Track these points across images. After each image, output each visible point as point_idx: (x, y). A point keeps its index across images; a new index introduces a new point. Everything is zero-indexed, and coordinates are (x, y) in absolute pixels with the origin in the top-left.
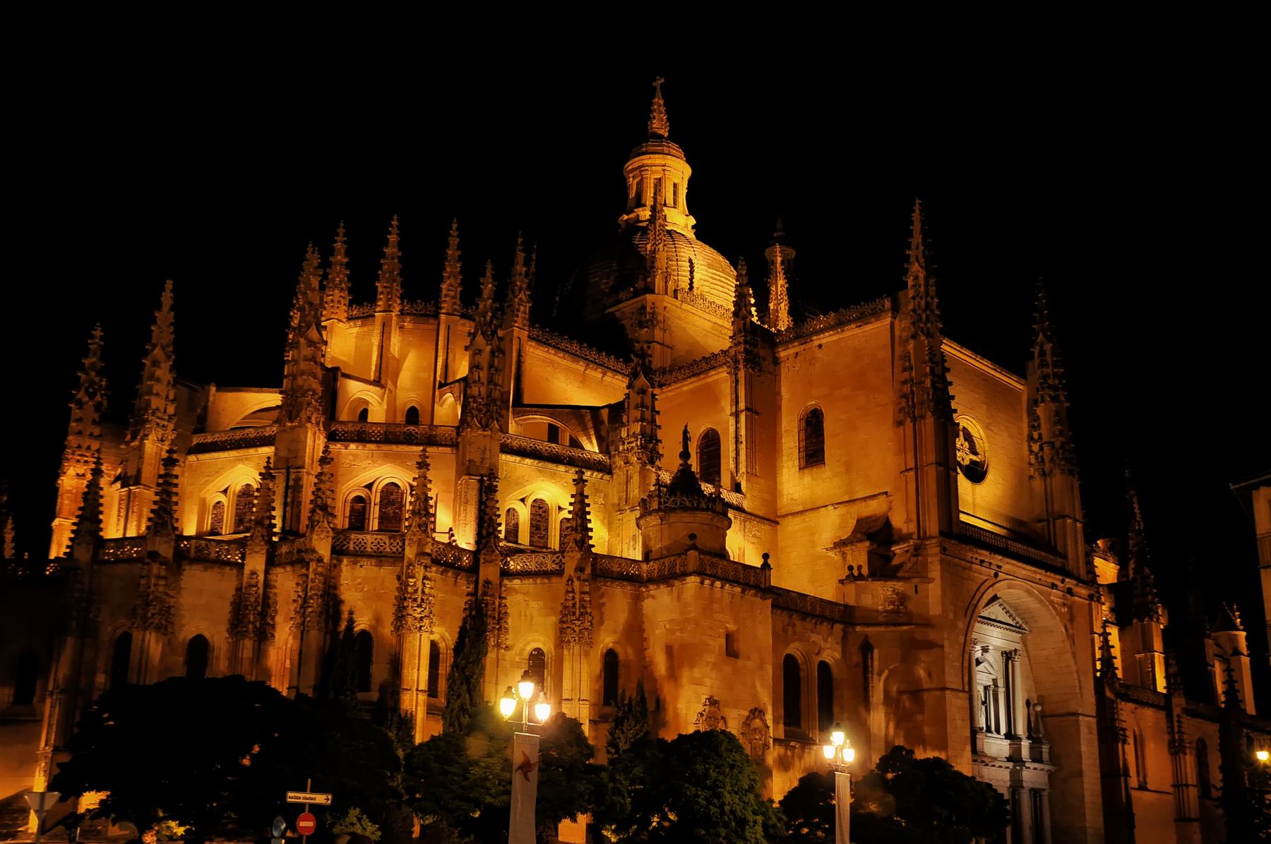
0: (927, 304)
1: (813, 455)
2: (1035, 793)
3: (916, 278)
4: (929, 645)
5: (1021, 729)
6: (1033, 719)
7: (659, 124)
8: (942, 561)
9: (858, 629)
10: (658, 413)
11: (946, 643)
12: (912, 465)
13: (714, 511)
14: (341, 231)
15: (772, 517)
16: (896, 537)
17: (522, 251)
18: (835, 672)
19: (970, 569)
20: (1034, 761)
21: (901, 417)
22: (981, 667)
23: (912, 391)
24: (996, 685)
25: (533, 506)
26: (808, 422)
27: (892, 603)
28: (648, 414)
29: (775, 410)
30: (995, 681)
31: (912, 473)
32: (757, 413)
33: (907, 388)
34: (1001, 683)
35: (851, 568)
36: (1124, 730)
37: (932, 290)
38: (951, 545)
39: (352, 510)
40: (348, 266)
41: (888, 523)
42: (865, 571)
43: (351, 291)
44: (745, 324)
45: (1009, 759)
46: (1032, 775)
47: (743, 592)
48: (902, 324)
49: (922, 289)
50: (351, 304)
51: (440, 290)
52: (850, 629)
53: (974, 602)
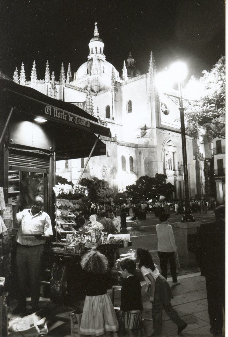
1: (130, 110)
2: (180, 182)
3: (151, 70)
4: (154, 152)
5: (177, 168)
6: (180, 166)
7: (96, 33)
9: (139, 149)
10: (93, 103)
11: (158, 151)
14: (23, 64)
16: (147, 128)
17: (63, 67)
18: (134, 158)
19: (164, 135)
20: (179, 175)
21: (148, 102)
22: (167, 156)
23: (150, 96)
24: (171, 160)
26: (128, 103)
28: (91, 104)
30: (171, 158)
32: (117, 102)
34: (172, 159)
36: (201, 167)
38: (159, 130)
40: (25, 73)
42: (140, 136)
43: (26, 78)
44: (114, 81)
45: (174, 175)
46: (179, 178)
50: (26, 81)
51: (45, 77)
52: (137, 149)
53: (165, 142)
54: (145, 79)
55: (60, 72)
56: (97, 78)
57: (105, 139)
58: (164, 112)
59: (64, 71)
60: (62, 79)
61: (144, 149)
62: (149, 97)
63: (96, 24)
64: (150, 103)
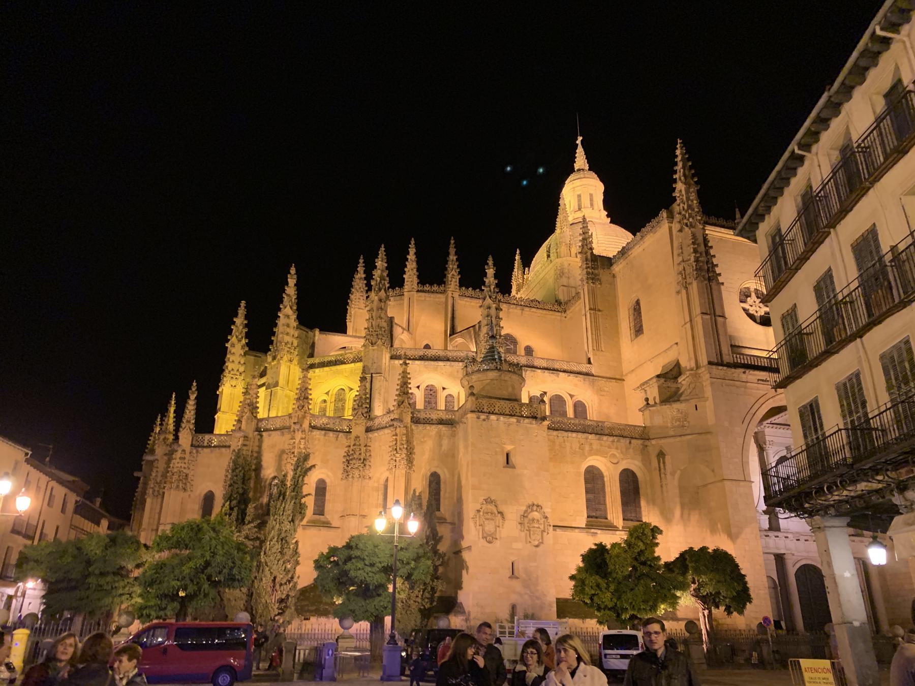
0: (689, 207)
1: (638, 330)
7: (581, 160)
8: (712, 384)
9: (653, 442)
12: (688, 319)
13: (500, 370)
14: (361, 261)
15: (617, 377)
18: (639, 474)
19: (746, 387)
21: (678, 288)
25: (426, 390)
26: (635, 309)
27: (679, 420)
29: (614, 307)
31: (688, 325)
32: (599, 311)
33: (681, 268)
35: (647, 399)
37: (693, 196)
39: (320, 408)
41: (678, 364)
42: (658, 401)
47: (518, 421)
48: (676, 226)
49: (684, 198)
52: (647, 443)
53: (753, 411)
54: (665, 225)
55: (446, 262)
56: (566, 266)
57: (496, 411)
58: (758, 321)
59: (455, 258)
60: (450, 276)
61: (671, 440)
62: (680, 273)
63: (580, 139)
64: (684, 292)
